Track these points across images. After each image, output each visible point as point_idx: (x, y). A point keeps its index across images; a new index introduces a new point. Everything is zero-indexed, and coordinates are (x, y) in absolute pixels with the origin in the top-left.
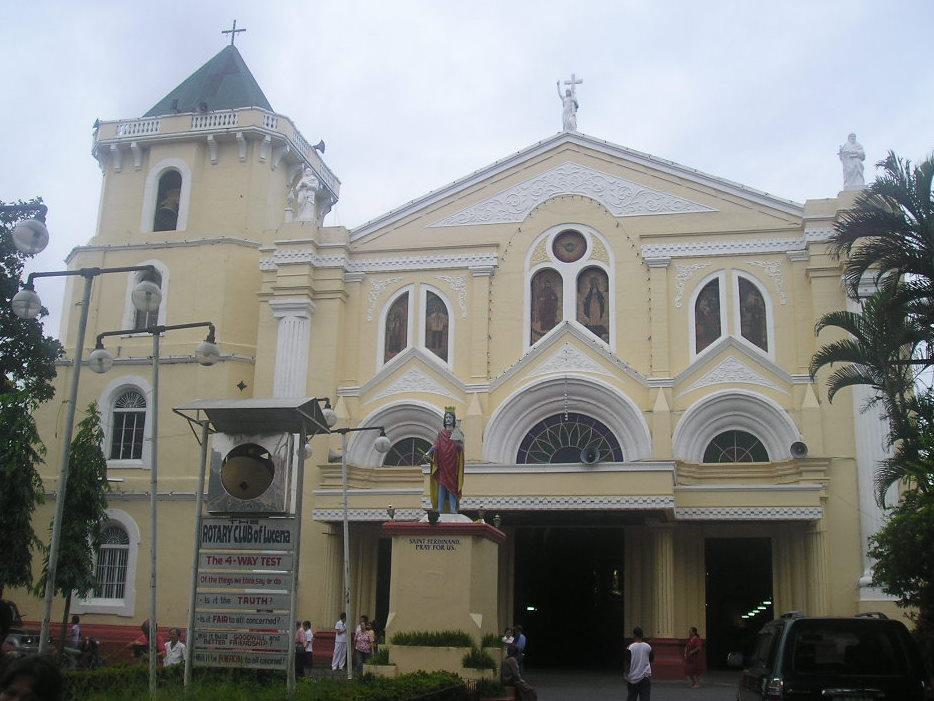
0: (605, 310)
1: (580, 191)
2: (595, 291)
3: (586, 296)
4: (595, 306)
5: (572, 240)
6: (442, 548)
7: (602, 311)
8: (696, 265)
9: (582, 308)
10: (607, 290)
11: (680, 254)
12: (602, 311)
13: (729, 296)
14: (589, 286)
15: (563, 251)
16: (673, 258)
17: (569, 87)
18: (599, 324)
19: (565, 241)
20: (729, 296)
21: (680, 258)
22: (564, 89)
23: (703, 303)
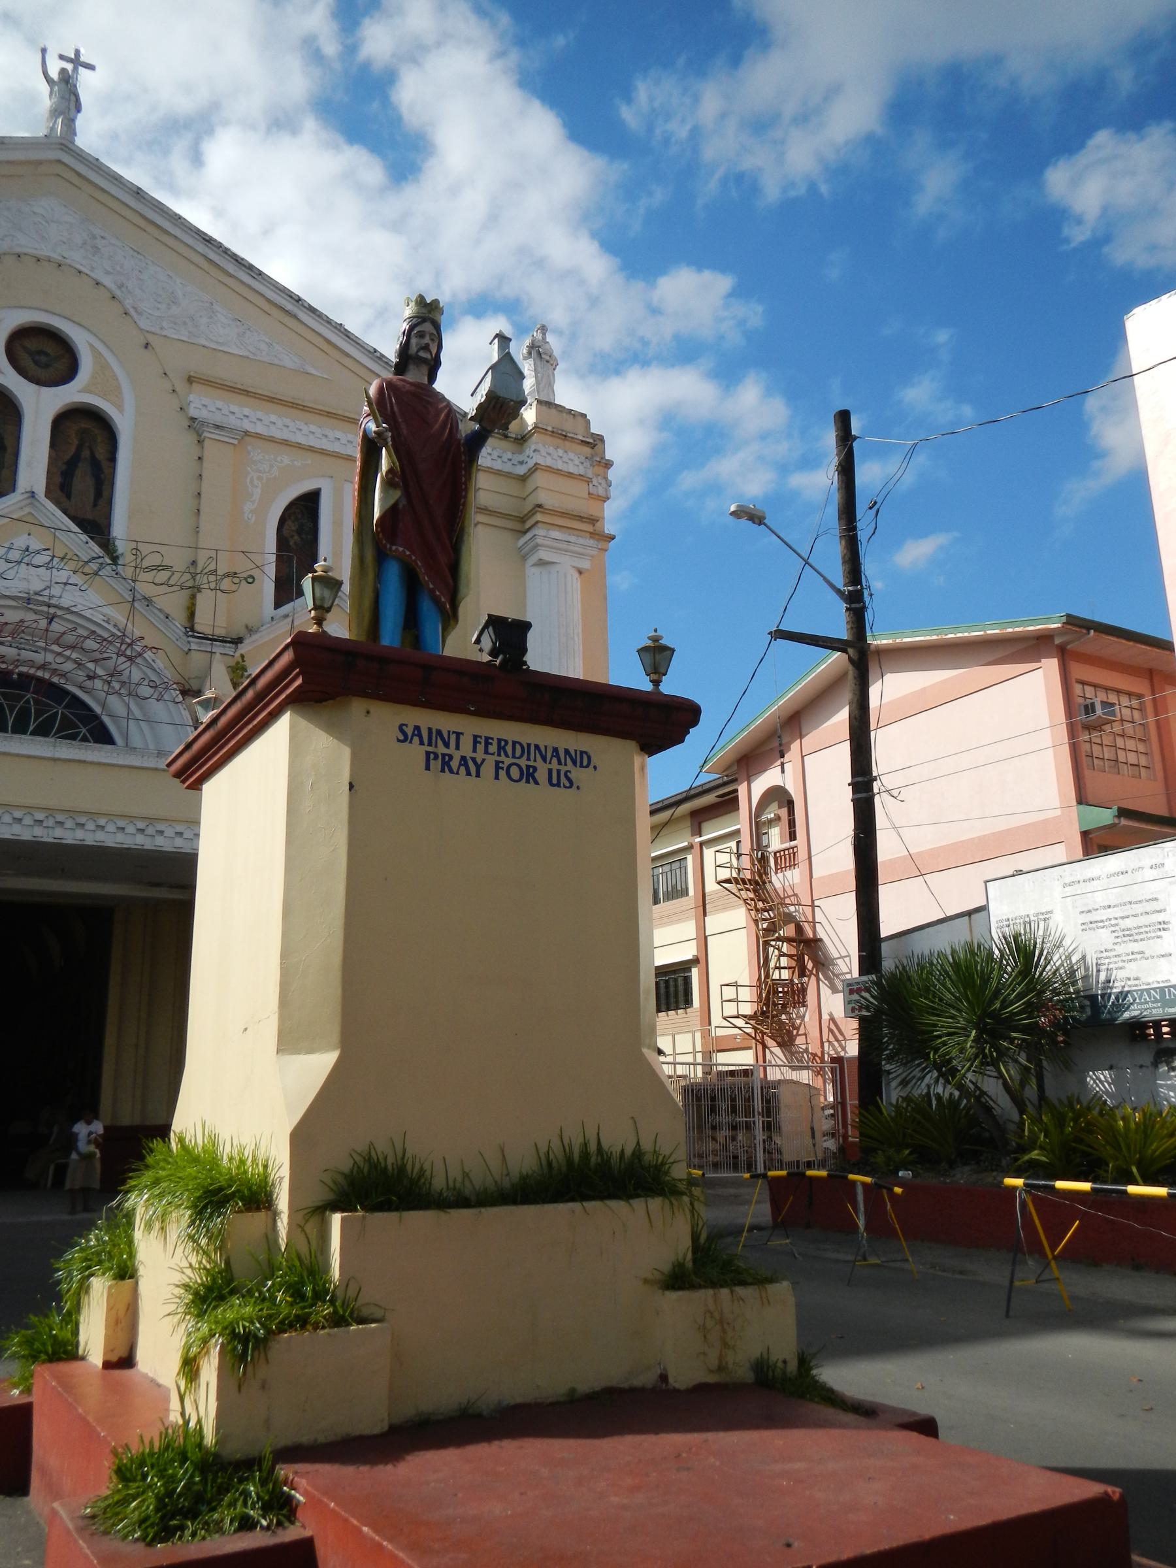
0: (105, 494)
1: (77, 258)
2: (86, 454)
3: (67, 457)
4: (83, 482)
5: (51, 348)
6: (529, 775)
7: (98, 494)
8: (286, 458)
9: (58, 479)
10: (113, 459)
11: (260, 429)
12: (98, 494)
13: (338, 524)
14: (76, 442)
15: (27, 361)
16: (246, 433)
17: (69, 67)
18: (89, 516)
19: (32, 344)
20: (338, 524)
21: (258, 436)
22: (54, 68)
23: (291, 526)
